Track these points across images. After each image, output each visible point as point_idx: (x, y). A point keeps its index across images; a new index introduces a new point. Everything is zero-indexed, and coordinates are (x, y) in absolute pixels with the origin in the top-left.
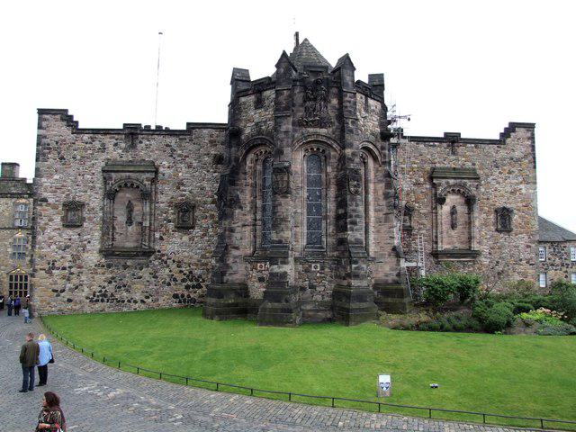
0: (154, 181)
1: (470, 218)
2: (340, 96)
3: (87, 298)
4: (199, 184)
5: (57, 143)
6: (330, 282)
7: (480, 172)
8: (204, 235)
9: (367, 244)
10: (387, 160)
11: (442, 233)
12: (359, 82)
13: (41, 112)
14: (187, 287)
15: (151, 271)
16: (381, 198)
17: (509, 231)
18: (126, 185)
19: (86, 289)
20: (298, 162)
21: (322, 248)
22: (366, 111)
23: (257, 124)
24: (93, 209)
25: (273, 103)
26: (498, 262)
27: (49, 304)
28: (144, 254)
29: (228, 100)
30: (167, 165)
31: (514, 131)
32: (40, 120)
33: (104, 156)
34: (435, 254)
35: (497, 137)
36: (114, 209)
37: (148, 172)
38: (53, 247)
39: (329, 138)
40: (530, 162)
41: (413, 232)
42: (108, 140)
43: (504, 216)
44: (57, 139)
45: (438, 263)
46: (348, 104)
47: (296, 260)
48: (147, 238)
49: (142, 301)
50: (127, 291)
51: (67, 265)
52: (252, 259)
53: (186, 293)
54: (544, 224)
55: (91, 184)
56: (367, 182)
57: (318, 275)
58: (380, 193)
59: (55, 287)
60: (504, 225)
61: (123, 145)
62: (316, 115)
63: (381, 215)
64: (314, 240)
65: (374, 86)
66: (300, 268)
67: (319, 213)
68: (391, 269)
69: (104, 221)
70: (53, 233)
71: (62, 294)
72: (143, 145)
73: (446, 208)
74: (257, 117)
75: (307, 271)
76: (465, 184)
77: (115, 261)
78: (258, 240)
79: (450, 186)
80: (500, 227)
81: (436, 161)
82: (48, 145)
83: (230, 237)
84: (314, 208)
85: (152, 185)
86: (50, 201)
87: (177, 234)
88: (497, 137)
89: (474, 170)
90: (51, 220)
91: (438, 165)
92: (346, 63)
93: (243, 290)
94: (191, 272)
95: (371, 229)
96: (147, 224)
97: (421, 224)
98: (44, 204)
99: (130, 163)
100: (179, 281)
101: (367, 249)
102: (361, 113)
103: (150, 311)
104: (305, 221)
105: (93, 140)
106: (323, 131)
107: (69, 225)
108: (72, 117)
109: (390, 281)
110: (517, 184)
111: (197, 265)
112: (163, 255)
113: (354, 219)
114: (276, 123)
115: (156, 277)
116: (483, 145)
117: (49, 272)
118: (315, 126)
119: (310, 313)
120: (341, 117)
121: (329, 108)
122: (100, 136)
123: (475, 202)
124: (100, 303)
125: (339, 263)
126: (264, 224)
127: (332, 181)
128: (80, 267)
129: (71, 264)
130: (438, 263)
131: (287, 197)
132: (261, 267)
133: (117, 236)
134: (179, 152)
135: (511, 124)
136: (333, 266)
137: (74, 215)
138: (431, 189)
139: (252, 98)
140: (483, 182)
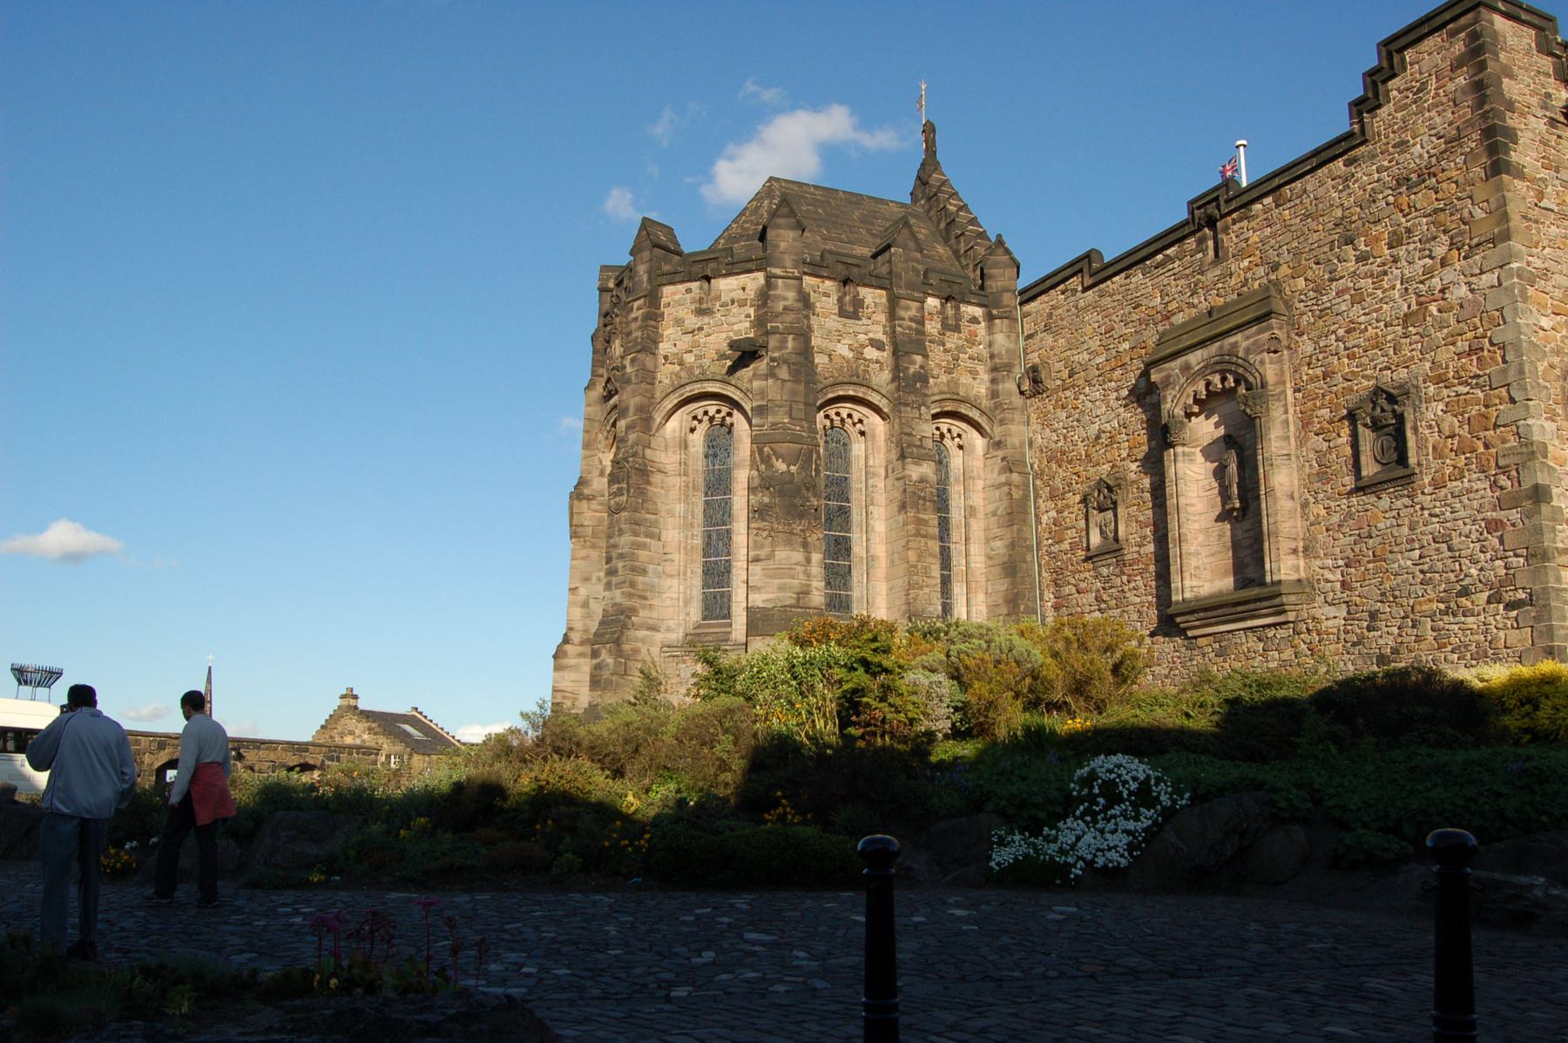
26: (1373, 616)
76: (1232, 352)
91: (1179, 319)
110: (1429, 273)
116: (1298, 184)
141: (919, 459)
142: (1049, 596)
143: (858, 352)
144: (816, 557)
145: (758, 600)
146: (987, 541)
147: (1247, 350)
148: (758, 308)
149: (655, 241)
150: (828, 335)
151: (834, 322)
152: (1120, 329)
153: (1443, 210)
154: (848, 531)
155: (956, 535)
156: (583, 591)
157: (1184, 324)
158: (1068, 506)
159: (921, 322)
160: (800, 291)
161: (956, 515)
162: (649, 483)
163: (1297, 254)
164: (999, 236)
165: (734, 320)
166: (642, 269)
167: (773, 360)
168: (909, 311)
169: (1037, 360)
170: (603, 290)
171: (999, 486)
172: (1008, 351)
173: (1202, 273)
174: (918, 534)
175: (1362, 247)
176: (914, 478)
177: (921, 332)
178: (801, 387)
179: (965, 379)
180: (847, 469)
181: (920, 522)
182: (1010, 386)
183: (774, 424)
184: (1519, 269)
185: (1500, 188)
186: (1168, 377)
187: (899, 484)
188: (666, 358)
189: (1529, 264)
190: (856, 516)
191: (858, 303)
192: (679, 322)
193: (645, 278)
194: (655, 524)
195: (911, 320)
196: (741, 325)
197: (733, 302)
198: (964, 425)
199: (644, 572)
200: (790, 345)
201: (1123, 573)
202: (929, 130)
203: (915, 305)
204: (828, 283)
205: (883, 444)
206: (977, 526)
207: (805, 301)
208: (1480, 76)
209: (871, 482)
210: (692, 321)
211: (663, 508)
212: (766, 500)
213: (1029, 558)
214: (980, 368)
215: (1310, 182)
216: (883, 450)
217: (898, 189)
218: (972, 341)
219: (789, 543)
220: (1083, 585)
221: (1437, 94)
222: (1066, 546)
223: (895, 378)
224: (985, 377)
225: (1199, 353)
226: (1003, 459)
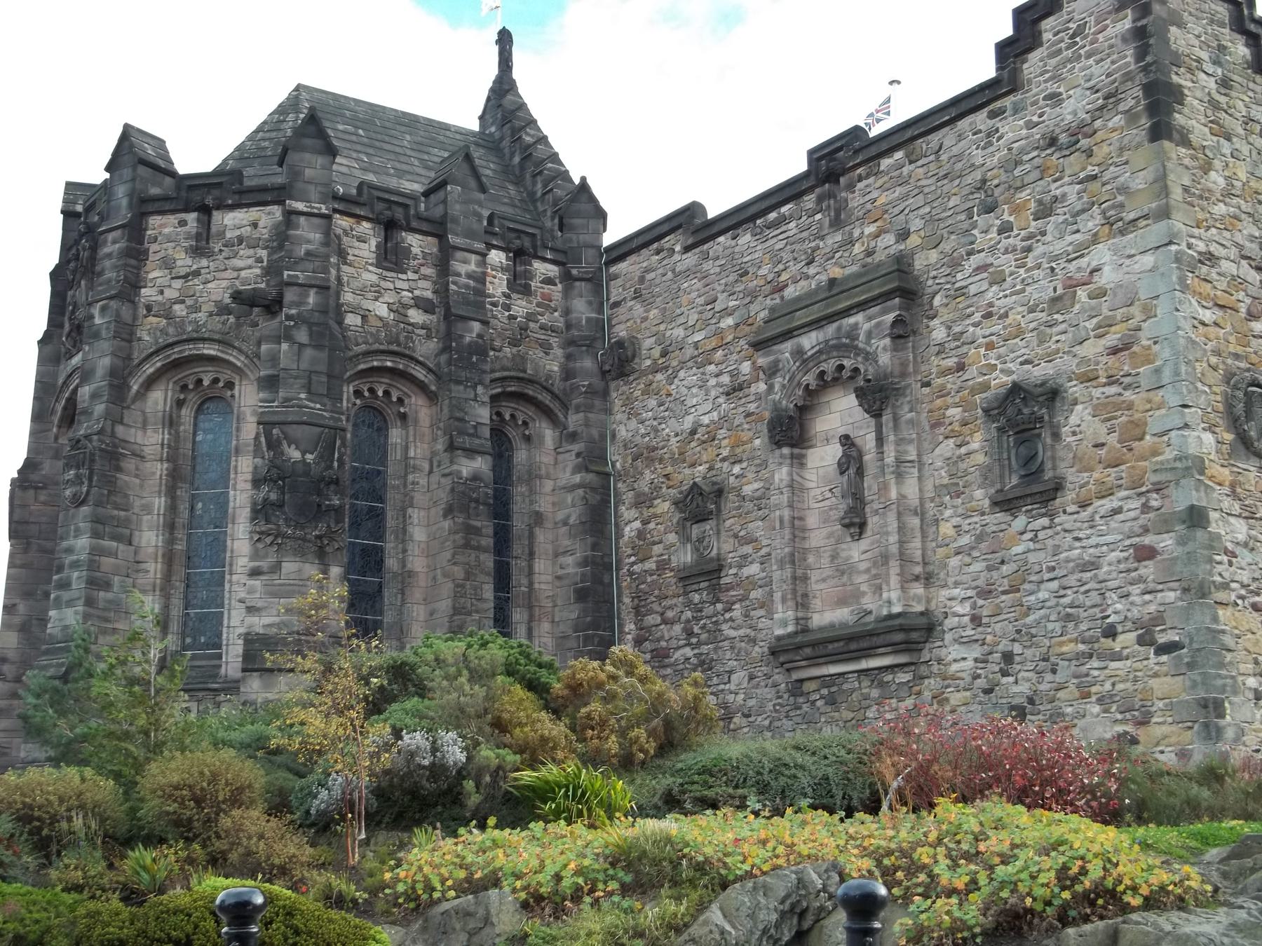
26: (1008, 657)
76: (852, 334)
81: (783, 278)
88: (987, 70)
91: (790, 292)
97: (749, 547)
110: (1081, 251)
116: (935, 138)
130: (797, 689)
140: (937, 301)
141: (471, 452)
142: (630, 627)
143: (399, 310)
144: (335, 571)
145: (259, 623)
146: (556, 555)
147: (869, 335)
148: (272, 251)
149: (135, 153)
150: (362, 292)
151: (370, 276)
153: (1094, 177)
154: (381, 537)
155: (518, 549)
156: (22, 608)
157: (798, 299)
158: (655, 516)
159: (481, 279)
160: (327, 232)
161: (519, 523)
162: (119, 469)
163: (930, 220)
164: (583, 179)
165: (238, 263)
166: (121, 191)
167: (289, 318)
168: (465, 266)
169: (623, 334)
170: (68, 214)
171: (572, 488)
172: (588, 320)
173: (822, 238)
174: (467, 545)
175: (1006, 217)
176: (465, 473)
177: (481, 293)
178: (324, 355)
179: (536, 354)
180: (383, 460)
181: (470, 530)
182: (588, 363)
183: (287, 400)
184: (1177, 252)
185: (1162, 158)
186: (777, 362)
187: (447, 482)
188: (149, 308)
189: (1190, 246)
190: (391, 522)
191: (407, 252)
192: (168, 264)
193: (124, 202)
194: (126, 523)
195: (469, 276)
196: (247, 269)
197: (240, 240)
198: (531, 411)
199: (107, 586)
200: (311, 300)
201: (718, 601)
202: (505, 39)
203: (474, 257)
204: (366, 225)
205: (427, 431)
206: (541, 536)
207: (335, 247)
208: (1144, 22)
209: (410, 478)
210: (184, 262)
211: (138, 503)
212: (273, 496)
213: (606, 581)
214: (554, 341)
215: (946, 137)
216: (427, 438)
217: (464, 111)
218: (546, 305)
219: (300, 553)
220: (670, 614)
221: (1096, 41)
222: (651, 565)
223: (446, 349)
224: (558, 352)
225: (813, 334)
226: (578, 455)
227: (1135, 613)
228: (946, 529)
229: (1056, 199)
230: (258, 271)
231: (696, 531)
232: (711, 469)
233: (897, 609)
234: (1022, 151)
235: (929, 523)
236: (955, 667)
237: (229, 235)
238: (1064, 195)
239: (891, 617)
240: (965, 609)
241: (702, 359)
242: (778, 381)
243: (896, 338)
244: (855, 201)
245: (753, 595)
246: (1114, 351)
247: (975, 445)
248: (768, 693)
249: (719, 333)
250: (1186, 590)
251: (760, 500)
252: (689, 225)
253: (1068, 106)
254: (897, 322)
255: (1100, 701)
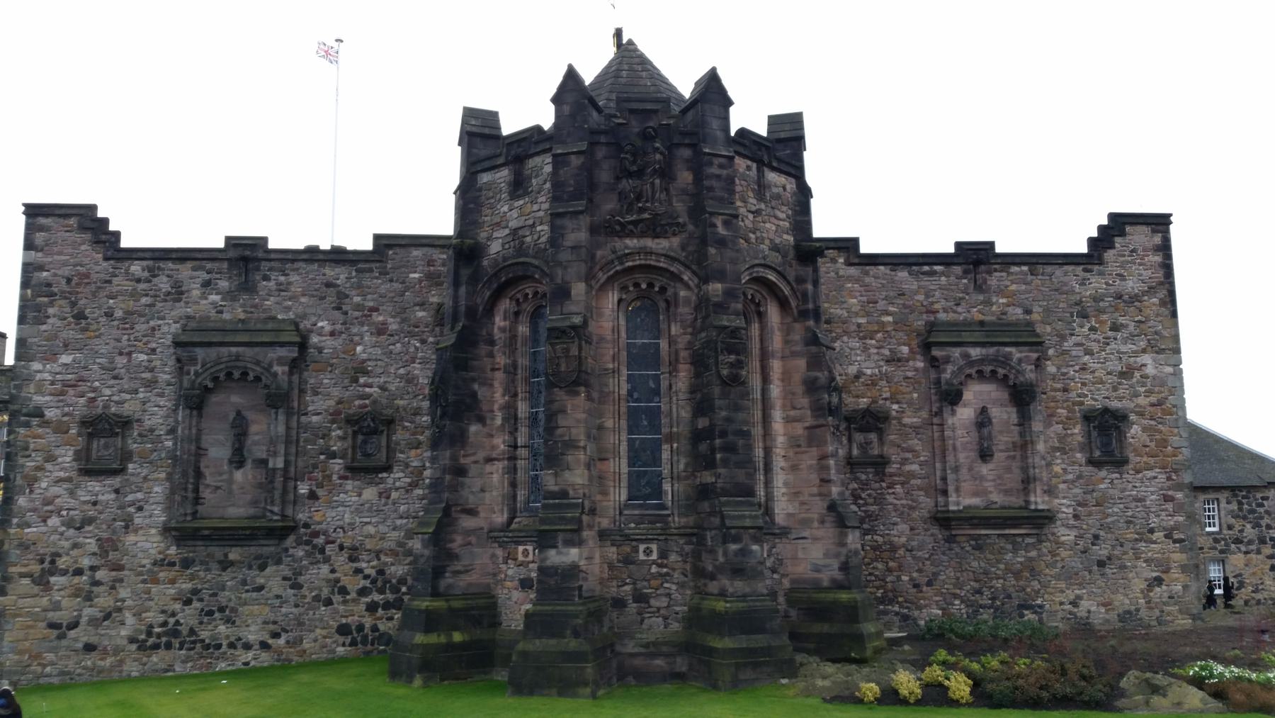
0: (296, 365)
1: (1022, 434)
2: (698, 165)
3: (132, 640)
4: (402, 371)
5: (69, 281)
6: (681, 585)
7: (1044, 330)
8: (414, 485)
9: (769, 497)
10: (811, 306)
11: (956, 469)
12: (743, 132)
13: (33, 211)
14: (372, 608)
15: (288, 573)
16: (800, 389)
17: (1119, 463)
18: (229, 375)
19: (130, 619)
20: (609, 316)
21: (663, 507)
22: (760, 196)
23: (515, 231)
24: (152, 430)
25: (548, 185)
26: (1096, 537)
27: (38, 656)
28: (271, 533)
29: (455, 180)
30: (328, 328)
31: (1122, 234)
32: (30, 230)
33: (181, 310)
34: (943, 520)
35: (1083, 248)
36: (199, 431)
37: (282, 344)
38: (54, 521)
39: (673, 259)
40: (1163, 303)
41: (892, 468)
42: (185, 271)
43: (1105, 428)
44: (66, 271)
45: (951, 539)
46: (715, 183)
47: (603, 535)
48: (277, 494)
49: (264, 646)
50: (229, 621)
51: (86, 562)
52: (504, 536)
53: (368, 622)
54: (1205, 442)
55: (147, 375)
56: (765, 356)
57: (654, 569)
58: (797, 378)
59: (54, 616)
60: (1106, 447)
61: (224, 284)
62: (642, 210)
63: (799, 429)
64: (644, 487)
65: (779, 141)
66: (612, 553)
67: (656, 428)
68: (826, 555)
69: (174, 458)
70: (56, 490)
71: (72, 634)
72: (272, 284)
73: (965, 414)
74: (520, 218)
75: (628, 561)
76: (1008, 357)
77: (201, 550)
78: (521, 494)
79: (971, 363)
80: (1097, 453)
81: (936, 306)
82: (49, 285)
83: (454, 488)
84: (643, 418)
85: (291, 373)
86: (50, 414)
87: (349, 485)
88: (1083, 248)
89: (1030, 324)
90: (51, 458)
91: (942, 316)
92: (712, 91)
93: (483, 611)
94: (381, 572)
95: (779, 463)
96: (279, 463)
97: (908, 455)
98: (35, 421)
99: (242, 326)
100: (353, 595)
101: (768, 511)
102: (746, 204)
103: (283, 668)
104: (624, 447)
105: (153, 273)
106: (662, 244)
107: (90, 469)
108: (105, 221)
109: (825, 584)
110: (1135, 354)
111: (394, 553)
112: (316, 534)
113: (731, 438)
114: (553, 228)
115: (297, 586)
116: (1049, 269)
117: (42, 581)
118: (642, 235)
119: (638, 662)
120: (698, 212)
121: (673, 192)
122: (170, 265)
123: (1033, 398)
124: (162, 652)
125: (701, 541)
126: (535, 455)
127: (683, 354)
128: (119, 568)
129: (95, 562)
130: (951, 539)
131: (577, 394)
132: (526, 553)
133: (206, 494)
134: (357, 299)
135: (1113, 217)
136: (688, 548)
137: (106, 447)
138: (925, 370)
139: (504, 175)
140: (1051, 352)
147: (1020, 361)
148: (796, 213)
152: (881, 305)
157: (949, 324)
163: (1047, 311)
165: (783, 216)
197: (778, 197)
202: (618, 33)
215: (1059, 272)
227: (1164, 524)
228: (1057, 469)
229: (1122, 325)
230: (787, 224)
231: (858, 437)
232: (874, 402)
233: (1040, 507)
234: (1105, 295)
235: (1049, 465)
236: (1063, 538)
237: (775, 190)
238: (1126, 326)
239: (1036, 510)
240: (1071, 510)
241: (864, 335)
242: (950, 368)
243: (1037, 366)
244: (993, 281)
245: (913, 482)
246: (1153, 405)
247: (1076, 431)
248: (929, 539)
249: (883, 324)
250: (1188, 517)
251: (916, 428)
252: (848, 246)
253: (1130, 284)
254: (1038, 359)
255: (1145, 561)
